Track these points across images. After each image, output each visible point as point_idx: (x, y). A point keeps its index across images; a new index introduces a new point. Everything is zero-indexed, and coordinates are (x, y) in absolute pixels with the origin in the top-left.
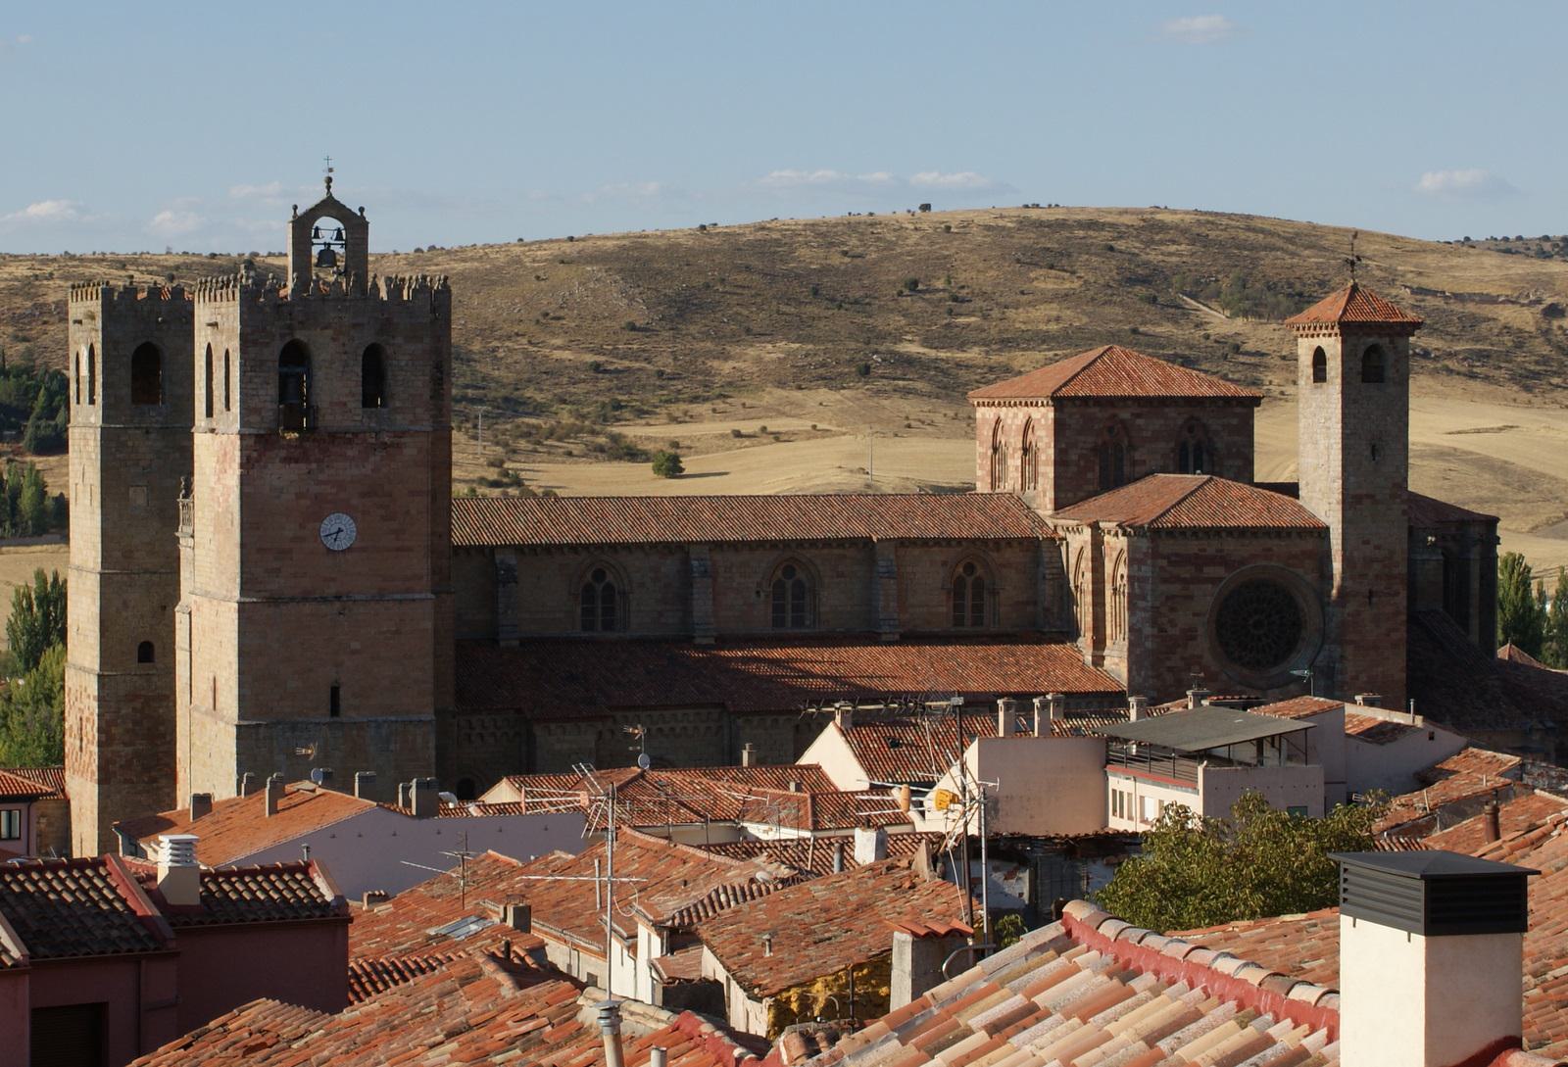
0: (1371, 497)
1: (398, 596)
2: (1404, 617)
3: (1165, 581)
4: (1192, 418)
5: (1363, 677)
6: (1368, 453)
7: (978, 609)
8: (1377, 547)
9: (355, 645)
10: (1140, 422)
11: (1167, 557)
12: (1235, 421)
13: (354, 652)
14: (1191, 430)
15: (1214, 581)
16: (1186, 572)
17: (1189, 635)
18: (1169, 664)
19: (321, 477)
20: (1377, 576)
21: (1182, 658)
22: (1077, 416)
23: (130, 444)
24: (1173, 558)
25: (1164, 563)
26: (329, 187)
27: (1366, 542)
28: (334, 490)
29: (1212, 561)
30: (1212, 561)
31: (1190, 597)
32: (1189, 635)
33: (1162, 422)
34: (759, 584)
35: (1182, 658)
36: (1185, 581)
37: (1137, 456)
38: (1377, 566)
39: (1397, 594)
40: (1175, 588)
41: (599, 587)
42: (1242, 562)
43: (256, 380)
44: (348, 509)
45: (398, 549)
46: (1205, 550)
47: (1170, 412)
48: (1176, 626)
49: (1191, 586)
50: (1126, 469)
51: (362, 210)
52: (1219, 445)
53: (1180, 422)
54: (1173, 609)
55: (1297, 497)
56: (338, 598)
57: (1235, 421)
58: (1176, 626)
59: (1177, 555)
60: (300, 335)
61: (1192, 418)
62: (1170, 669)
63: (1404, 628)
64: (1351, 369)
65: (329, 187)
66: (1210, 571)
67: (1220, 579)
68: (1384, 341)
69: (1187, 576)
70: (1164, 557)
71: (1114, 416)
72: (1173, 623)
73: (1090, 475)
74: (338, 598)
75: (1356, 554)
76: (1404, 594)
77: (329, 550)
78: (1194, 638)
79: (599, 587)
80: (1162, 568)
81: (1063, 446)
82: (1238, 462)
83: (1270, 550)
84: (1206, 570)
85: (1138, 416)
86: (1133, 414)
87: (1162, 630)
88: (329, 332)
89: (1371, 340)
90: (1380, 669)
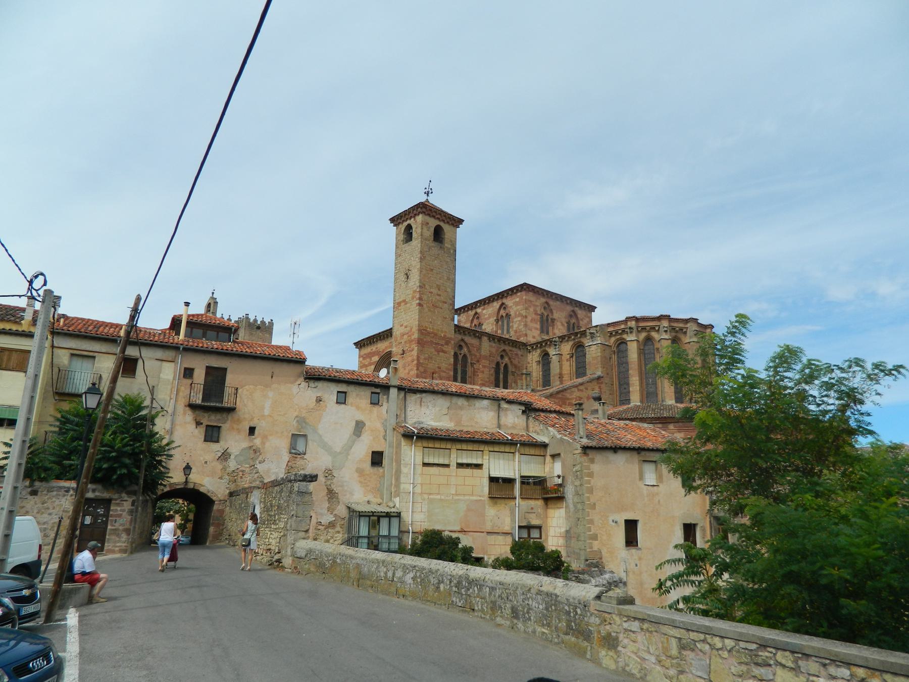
0: (404, 301)
8: (406, 327)
10: (484, 311)
11: (362, 356)
12: (517, 300)
27: (402, 326)
33: (492, 309)
38: (405, 337)
42: (383, 351)
46: (372, 350)
52: (512, 313)
53: (498, 307)
57: (517, 300)
61: (503, 304)
68: (411, 222)
70: (362, 356)
85: (484, 309)
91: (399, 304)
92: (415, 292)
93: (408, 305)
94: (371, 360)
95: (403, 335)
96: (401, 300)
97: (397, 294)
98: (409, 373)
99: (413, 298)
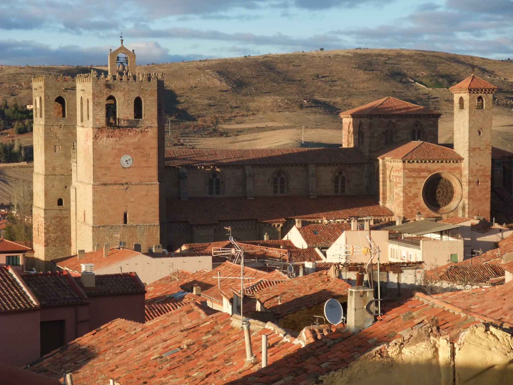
0: (479, 148)
1: (146, 183)
2: (490, 190)
3: (408, 177)
4: (417, 122)
5: (476, 210)
6: (478, 133)
7: (343, 187)
8: (481, 166)
9: (132, 200)
10: (399, 123)
12: (432, 123)
13: (132, 202)
14: (416, 126)
15: (424, 177)
16: (414, 174)
17: (416, 196)
18: (409, 206)
19: (120, 142)
20: (480, 176)
21: (414, 204)
22: (378, 121)
23: (55, 131)
24: (410, 170)
25: (407, 171)
26: (122, 43)
27: (477, 164)
28: (125, 147)
29: (423, 171)
30: (423, 171)
31: (416, 183)
32: (416, 196)
34: (269, 179)
35: (414, 204)
36: (414, 177)
37: (398, 135)
38: (480, 172)
39: (487, 182)
40: (411, 180)
41: (214, 180)
42: (434, 171)
43: (97, 109)
44: (129, 153)
45: (147, 167)
46: (421, 167)
47: (410, 120)
48: (411, 193)
49: (417, 179)
50: (394, 139)
51: (133, 51)
54: (410, 187)
55: (453, 148)
56: (127, 183)
58: (411, 193)
59: (411, 168)
60: (113, 94)
61: (417, 122)
62: (409, 207)
63: (490, 193)
64: (472, 104)
65: (122, 43)
66: (423, 174)
67: (426, 177)
69: (415, 175)
70: (407, 169)
71: (390, 121)
72: (410, 192)
73: (382, 141)
74: (127, 183)
75: (473, 168)
76: (490, 182)
77: (124, 168)
78: (417, 197)
79: (214, 180)
80: (407, 173)
81: (373, 131)
82: (433, 137)
83: (443, 167)
84: (421, 173)
85: (399, 121)
86: (396, 120)
87: (407, 194)
88: (123, 93)
89: (480, 95)
90: (481, 207)
91: (474, 149)
92: (488, 145)
93: (482, 152)
94: (420, 174)
95: (479, 170)
96: (476, 146)
97: (472, 142)
98: (484, 196)
99: (486, 148)
